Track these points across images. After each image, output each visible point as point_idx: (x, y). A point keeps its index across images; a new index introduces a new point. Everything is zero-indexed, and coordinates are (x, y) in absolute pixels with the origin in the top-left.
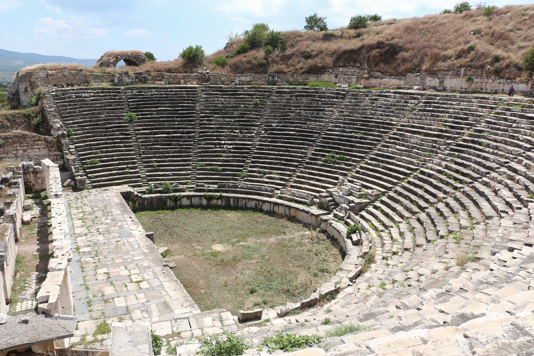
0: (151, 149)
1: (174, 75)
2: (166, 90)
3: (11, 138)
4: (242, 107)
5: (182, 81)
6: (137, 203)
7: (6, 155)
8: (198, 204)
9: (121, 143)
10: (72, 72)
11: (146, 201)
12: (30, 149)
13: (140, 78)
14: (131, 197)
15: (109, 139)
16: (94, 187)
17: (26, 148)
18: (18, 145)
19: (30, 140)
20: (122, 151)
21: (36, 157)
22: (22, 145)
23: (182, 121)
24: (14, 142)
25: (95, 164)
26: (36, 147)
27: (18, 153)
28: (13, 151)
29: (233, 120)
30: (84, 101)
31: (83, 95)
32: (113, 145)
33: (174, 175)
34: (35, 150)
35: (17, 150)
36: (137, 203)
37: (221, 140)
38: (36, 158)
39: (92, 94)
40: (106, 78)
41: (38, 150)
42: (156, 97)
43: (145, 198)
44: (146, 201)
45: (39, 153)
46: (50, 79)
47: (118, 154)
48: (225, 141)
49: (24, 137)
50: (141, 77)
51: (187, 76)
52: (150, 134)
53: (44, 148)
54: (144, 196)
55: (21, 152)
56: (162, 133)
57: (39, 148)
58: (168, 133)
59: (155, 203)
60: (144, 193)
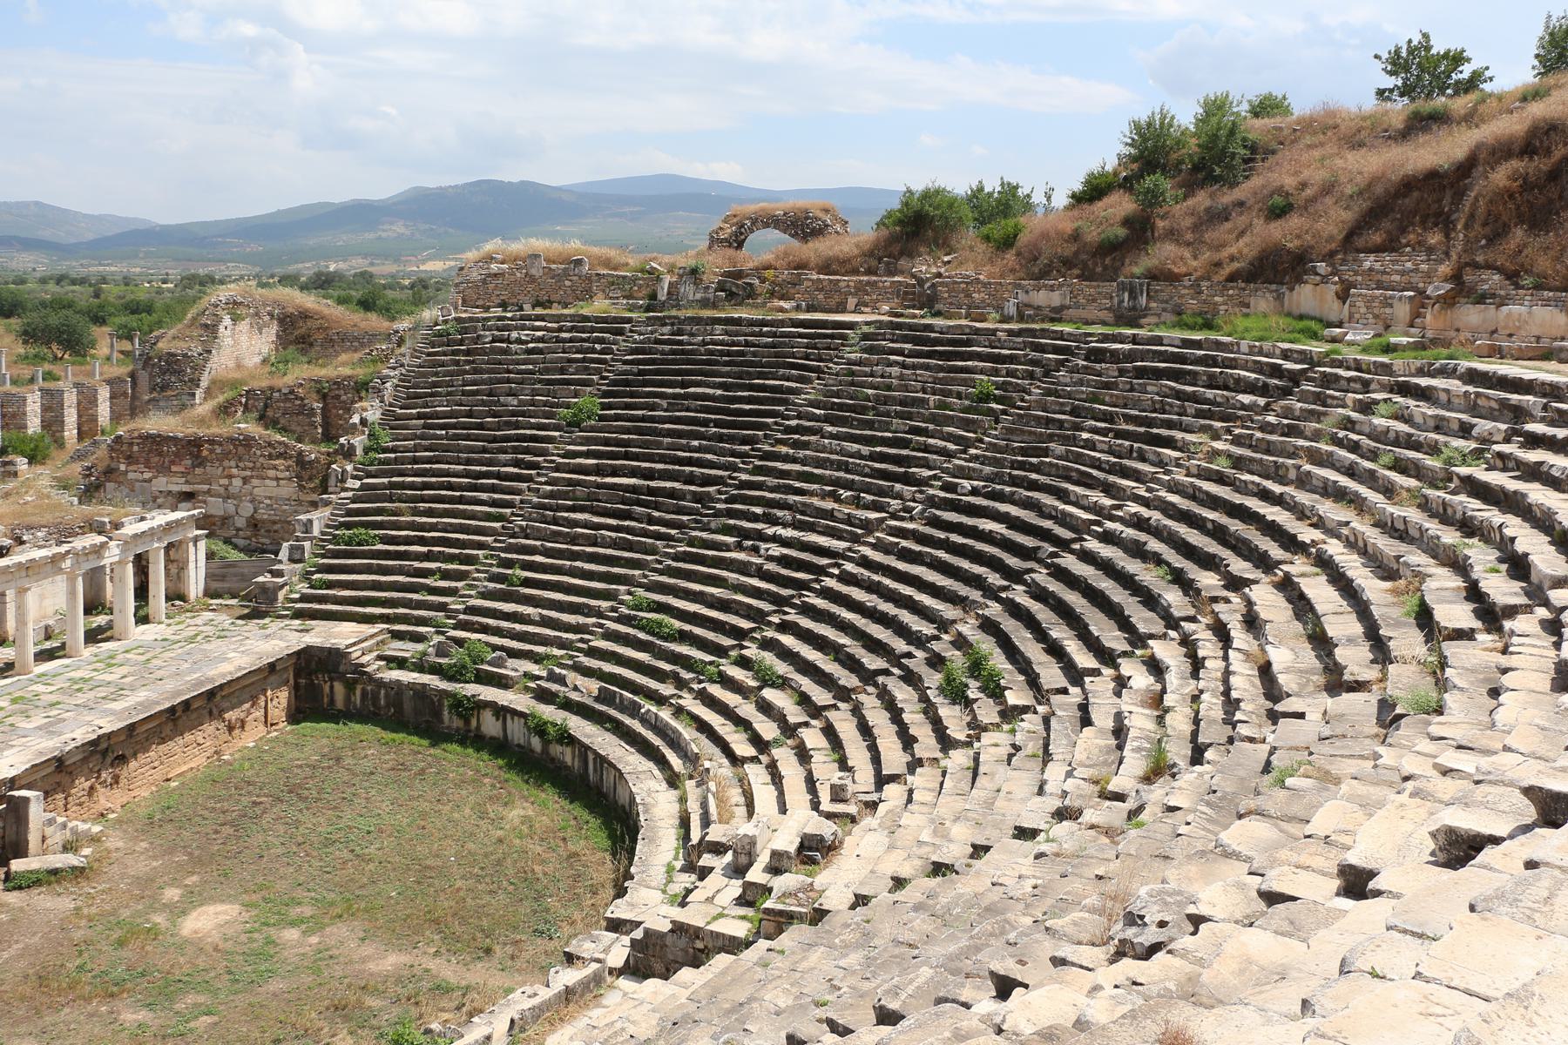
0: (555, 522)
1: (831, 281)
2: (757, 329)
3: (220, 444)
4: (931, 404)
5: (852, 302)
6: (358, 692)
7: (206, 487)
8: (522, 742)
9: (493, 489)
10: (553, 266)
11: (383, 692)
12: (257, 477)
13: (734, 289)
14: (342, 668)
15: (467, 475)
16: (299, 614)
18: (233, 463)
19: (258, 453)
20: (473, 516)
21: (268, 502)
22: (241, 464)
23: (721, 438)
24: (226, 455)
25: (359, 544)
26: (272, 473)
27: (230, 484)
28: (221, 477)
29: (865, 450)
30: (505, 352)
31: (514, 335)
32: (458, 494)
33: (546, 622)
34: (267, 481)
35: (230, 477)
36: (358, 692)
37: (774, 521)
38: (268, 505)
39: (540, 334)
40: (640, 287)
41: (275, 483)
42: (711, 353)
43: (380, 683)
44: (383, 692)
45: (275, 492)
46: (491, 286)
47: (451, 525)
48: (785, 525)
49: (247, 442)
50: (737, 286)
51: (868, 283)
52: (598, 471)
53: (290, 479)
55: (237, 482)
56: (633, 473)
57: (277, 479)
58: (649, 475)
59: (408, 706)
60: (401, 663)
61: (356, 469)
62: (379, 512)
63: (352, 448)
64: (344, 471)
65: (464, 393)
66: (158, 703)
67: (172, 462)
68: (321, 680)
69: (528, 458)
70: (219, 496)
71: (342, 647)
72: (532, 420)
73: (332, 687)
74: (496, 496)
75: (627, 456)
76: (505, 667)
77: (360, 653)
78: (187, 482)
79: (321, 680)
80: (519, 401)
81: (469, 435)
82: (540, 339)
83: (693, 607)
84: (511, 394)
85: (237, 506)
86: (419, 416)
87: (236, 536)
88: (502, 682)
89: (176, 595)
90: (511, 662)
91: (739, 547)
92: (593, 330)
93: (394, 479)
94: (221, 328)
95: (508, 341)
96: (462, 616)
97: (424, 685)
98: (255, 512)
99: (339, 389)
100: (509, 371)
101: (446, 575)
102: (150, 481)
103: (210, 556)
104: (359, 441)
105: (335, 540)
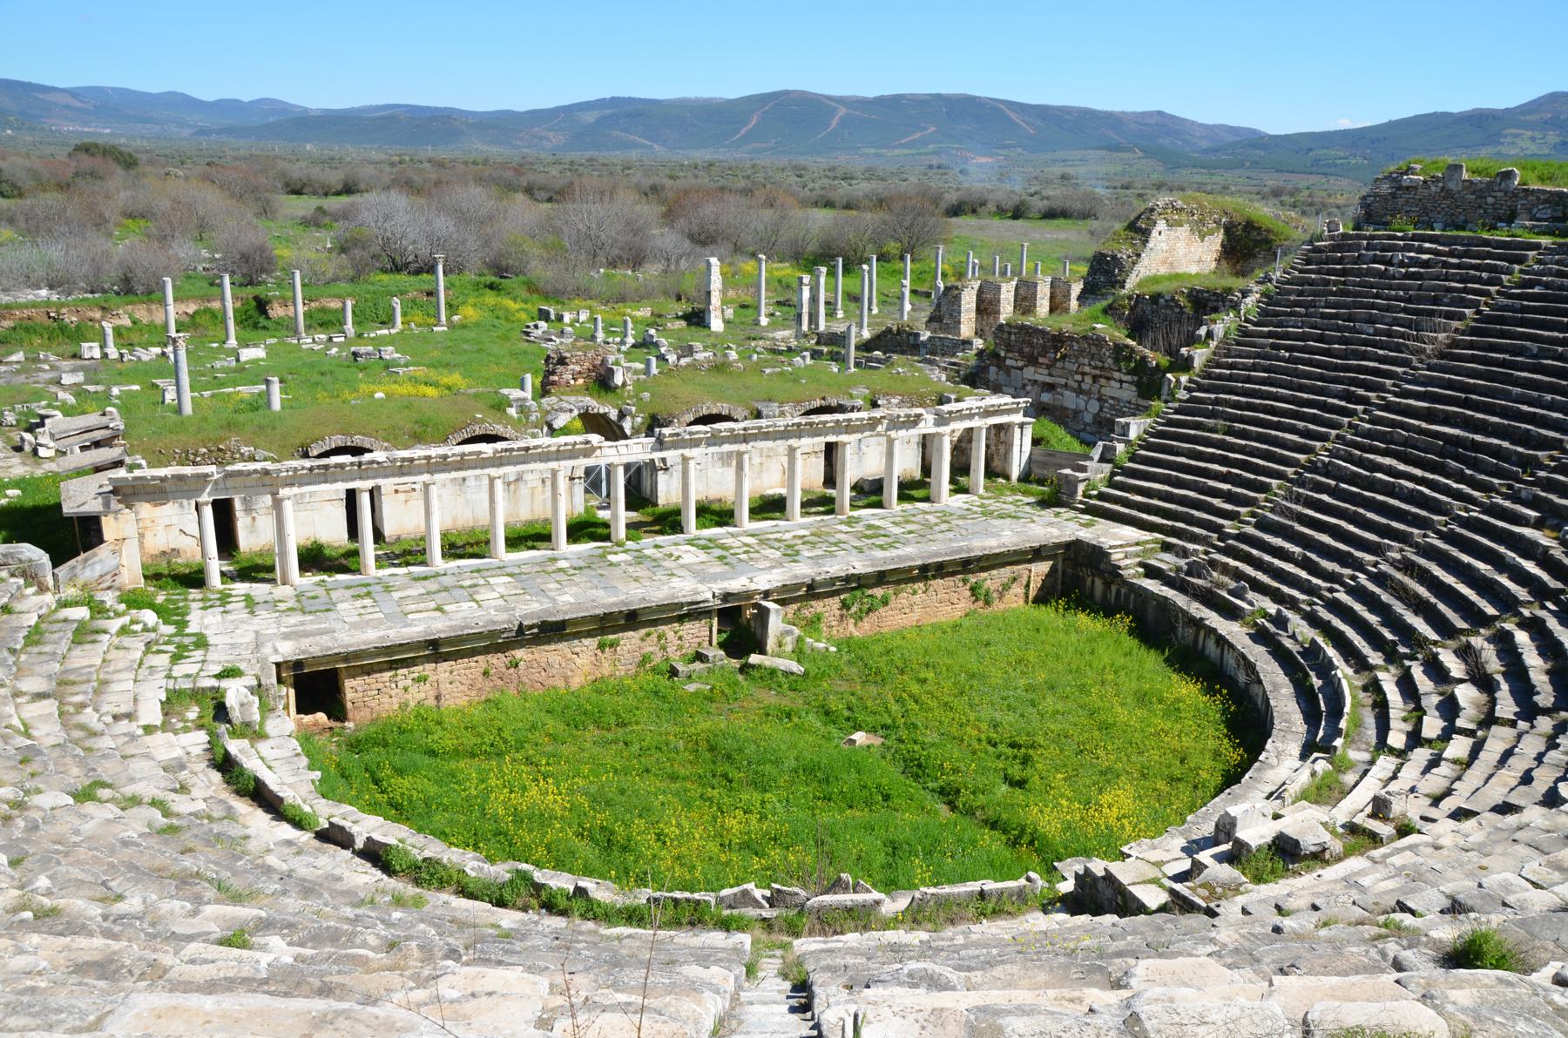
3: (1077, 341)
16: (1090, 510)
17: (1098, 372)
18: (1086, 361)
27: (1083, 380)
28: (1077, 373)
34: (1113, 383)
41: (1118, 385)
45: (1117, 394)
46: (1401, 201)
47: (1258, 449)
52: (1429, 416)
53: (1131, 383)
54: (1152, 585)
55: (1088, 379)
57: (1121, 382)
60: (1152, 572)
61: (1191, 381)
62: (1197, 426)
63: (1190, 359)
64: (1178, 381)
65: (1323, 316)
66: (912, 559)
67: (1040, 355)
68: (1084, 572)
69: (1361, 392)
70: (1074, 390)
71: (1105, 546)
72: (1381, 352)
73: (1093, 582)
74: (1311, 426)
75: (1467, 404)
76: (1243, 599)
77: (1122, 555)
78: (1050, 375)
79: (1084, 572)
80: (1376, 329)
81: (1311, 360)
82: (1426, 264)
83: (1449, 579)
84: (1371, 320)
85: (1087, 403)
86: (1270, 335)
87: (1084, 430)
88: (1231, 613)
89: (994, 472)
90: (1250, 595)
91: (1538, 525)
92: (1490, 256)
93: (1221, 396)
94: (1154, 233)
95: (1389, 262)
96: (1230, 542)
97: (1166, 598)
98: (1101, 410)
99: (1217, 301)
100: (1377, 296)
101: (1229, 497)
102: (1021, 369)
103: (1036, 442)
104: (1200, 355)
105: (1150, 447)
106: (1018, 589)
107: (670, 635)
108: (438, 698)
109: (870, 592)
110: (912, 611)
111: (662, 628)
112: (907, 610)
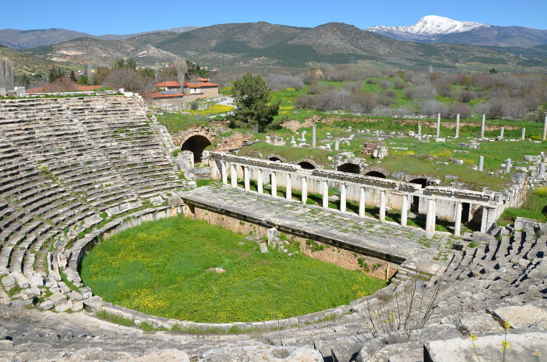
77: (405, 273)
106: (380, 271)
107: (257, 228)
108: (210, 220)
109: (316, 242)
110: (333, 258)
111: (255, 225)
112: (331, 256)
